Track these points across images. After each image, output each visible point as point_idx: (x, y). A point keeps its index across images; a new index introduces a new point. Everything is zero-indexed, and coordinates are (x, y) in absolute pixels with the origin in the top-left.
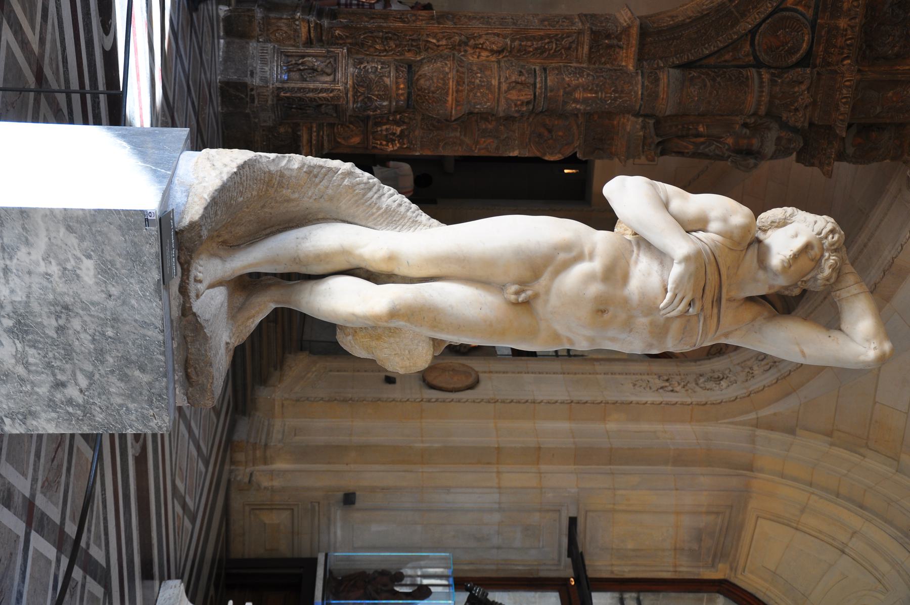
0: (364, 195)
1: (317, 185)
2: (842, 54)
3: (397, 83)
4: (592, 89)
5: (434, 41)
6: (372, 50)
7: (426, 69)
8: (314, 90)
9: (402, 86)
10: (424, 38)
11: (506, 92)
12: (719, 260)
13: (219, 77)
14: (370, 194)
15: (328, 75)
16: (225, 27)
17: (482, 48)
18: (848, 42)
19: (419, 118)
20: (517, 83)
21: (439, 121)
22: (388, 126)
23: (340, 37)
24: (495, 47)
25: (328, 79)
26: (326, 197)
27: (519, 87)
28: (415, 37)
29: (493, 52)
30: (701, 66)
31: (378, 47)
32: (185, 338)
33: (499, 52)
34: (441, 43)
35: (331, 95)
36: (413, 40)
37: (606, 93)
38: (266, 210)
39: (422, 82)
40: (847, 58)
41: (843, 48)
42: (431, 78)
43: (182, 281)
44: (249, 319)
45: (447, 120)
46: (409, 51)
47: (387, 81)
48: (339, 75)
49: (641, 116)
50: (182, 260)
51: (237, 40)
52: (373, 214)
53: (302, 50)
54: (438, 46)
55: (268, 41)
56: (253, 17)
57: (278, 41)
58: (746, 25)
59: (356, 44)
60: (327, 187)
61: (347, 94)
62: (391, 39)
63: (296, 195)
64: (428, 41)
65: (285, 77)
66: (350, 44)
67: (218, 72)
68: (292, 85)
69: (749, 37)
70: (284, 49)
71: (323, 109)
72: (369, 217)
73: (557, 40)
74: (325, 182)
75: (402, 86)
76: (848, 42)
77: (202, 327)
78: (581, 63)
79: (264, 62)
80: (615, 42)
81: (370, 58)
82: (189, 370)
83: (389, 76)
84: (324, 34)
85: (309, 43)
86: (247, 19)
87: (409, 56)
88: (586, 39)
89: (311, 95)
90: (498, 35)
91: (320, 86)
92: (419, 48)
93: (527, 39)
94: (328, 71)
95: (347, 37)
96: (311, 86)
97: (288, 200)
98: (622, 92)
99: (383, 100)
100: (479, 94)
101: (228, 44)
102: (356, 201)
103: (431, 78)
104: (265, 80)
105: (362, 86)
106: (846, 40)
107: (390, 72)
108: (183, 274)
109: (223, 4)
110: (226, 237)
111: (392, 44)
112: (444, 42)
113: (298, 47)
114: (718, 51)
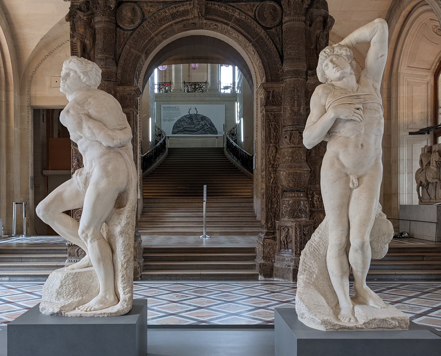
3: (292, 197)
4: (293, 102)
5: (272, 180)
6: (277, 209)
7: (285, 183)
8: (296, 238)
9: (293, 195)
10: (271, 184)
11: (295, 144)
13: (291, 282)
15: (289, 230)
16: (268, 277)
19: (310, 186)
20: (290, 139)
21: (311, 176)
22: (314, 201)
23: (272, 224)
24: (274, 151)
25: (291, 230)
27: (292, 138)
28: (270, 189)
29: (276, 152)
30: (282, 52)
31: (275, 206)
33: (277, 149)
35: (298, 228)
36: (272, 190)
37: (295, 95)
39: (291, 185)
42: (289, 181)
45: (311, 173)
46: (277, 191)
47: (291, 202)
48: (289, 224)
49: (307, 78)
51: (274, 272)
53: (278, 242)
54: (274, 178)
55: (274, 257)
56: (263, 264)
57: (274, 253)
58: (262, 33)
59: (275, 216)
61: (297, 221)
62: (271, 200)
65: (290, 250)
66: (275, 219)
67: (289, 282)
68: (294, 248)
69: (267, 30)
70: (277, 250)
71: (306, 232)
73: (270, 122)
75: (293, 195)
78: (281, 109)
79: (283, 260)
80: (271, 94)
81: (281, 210)
83: (289, 201)
84: (270, 231)
85: (274, 239)
86: (264, 267)
87: (279, 192)
88: (269, 108)
89: (298, 239)
90: (268, 150)
91: (294, 234)
92: (276, 187)
93: (270, 136)
94: (287, 230)
95: (271, 221)
96: (294, 238)
98: (294, 88)
99: (301, 203)
100: (296, 158)
101: (276, 276)
103: (289, 181)
104: (292, 260)
105: (294, 214)
107: (287, 201)
109: (258, 278)
111: (274, 200)
112: (272, 175)
113: (276, 244)
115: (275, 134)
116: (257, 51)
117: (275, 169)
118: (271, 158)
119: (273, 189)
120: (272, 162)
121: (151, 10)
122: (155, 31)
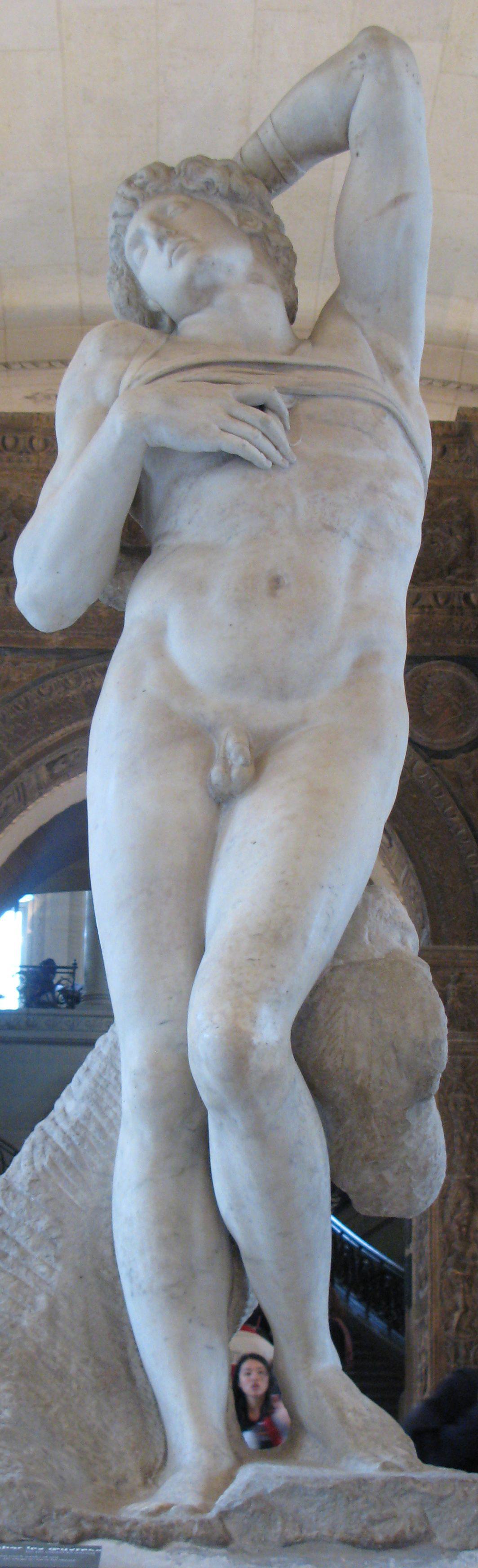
0: (57, 1149)
1: (24, 1254)
2: (460, 608)
5: (457, 1315)
10: (451, 1333)
12: (166, 366)
14: (56, 1136)
17: (468, 1226)
18: (441, 601)
24: (465, 1203)
26: (54, 1234)
32: (288, 1544)
34: (460, 1303)
36: (457, 1355)
38: (73, 1369)
40: (466, 597)
41: (453, 607)
43: (127, 1538)
44: (343, 1421)
50: (71, 1534)
52: (101, 1129)
54: (466, 1308)
60: (31, 1231)
63: (42, 1301)
64: (458, 1328)
72: (105, 1136)
74: (20, 1234)
76: (441, 601)
77: (258, 1498)
82: (380, 1538)
97: (52, 1316)
102: (70, 1166)
106: (439, 606)
108: (110, 1536)
110: (131, 1466)
114: (461, 809)
115: (467, 1137)
116: (399, 834)
117: (468, 1272)
118: (455, 1228)
119: (462, 1351)
120: (457, 1246)
121: (14, 678)
122: (24, 750)
